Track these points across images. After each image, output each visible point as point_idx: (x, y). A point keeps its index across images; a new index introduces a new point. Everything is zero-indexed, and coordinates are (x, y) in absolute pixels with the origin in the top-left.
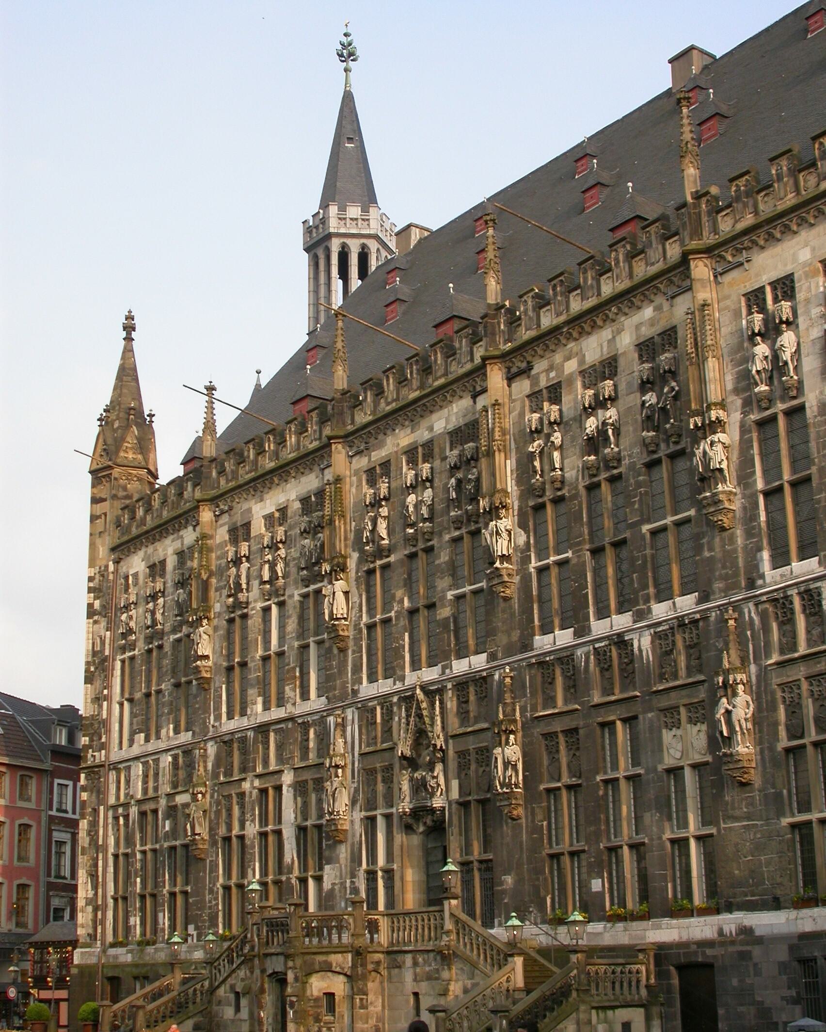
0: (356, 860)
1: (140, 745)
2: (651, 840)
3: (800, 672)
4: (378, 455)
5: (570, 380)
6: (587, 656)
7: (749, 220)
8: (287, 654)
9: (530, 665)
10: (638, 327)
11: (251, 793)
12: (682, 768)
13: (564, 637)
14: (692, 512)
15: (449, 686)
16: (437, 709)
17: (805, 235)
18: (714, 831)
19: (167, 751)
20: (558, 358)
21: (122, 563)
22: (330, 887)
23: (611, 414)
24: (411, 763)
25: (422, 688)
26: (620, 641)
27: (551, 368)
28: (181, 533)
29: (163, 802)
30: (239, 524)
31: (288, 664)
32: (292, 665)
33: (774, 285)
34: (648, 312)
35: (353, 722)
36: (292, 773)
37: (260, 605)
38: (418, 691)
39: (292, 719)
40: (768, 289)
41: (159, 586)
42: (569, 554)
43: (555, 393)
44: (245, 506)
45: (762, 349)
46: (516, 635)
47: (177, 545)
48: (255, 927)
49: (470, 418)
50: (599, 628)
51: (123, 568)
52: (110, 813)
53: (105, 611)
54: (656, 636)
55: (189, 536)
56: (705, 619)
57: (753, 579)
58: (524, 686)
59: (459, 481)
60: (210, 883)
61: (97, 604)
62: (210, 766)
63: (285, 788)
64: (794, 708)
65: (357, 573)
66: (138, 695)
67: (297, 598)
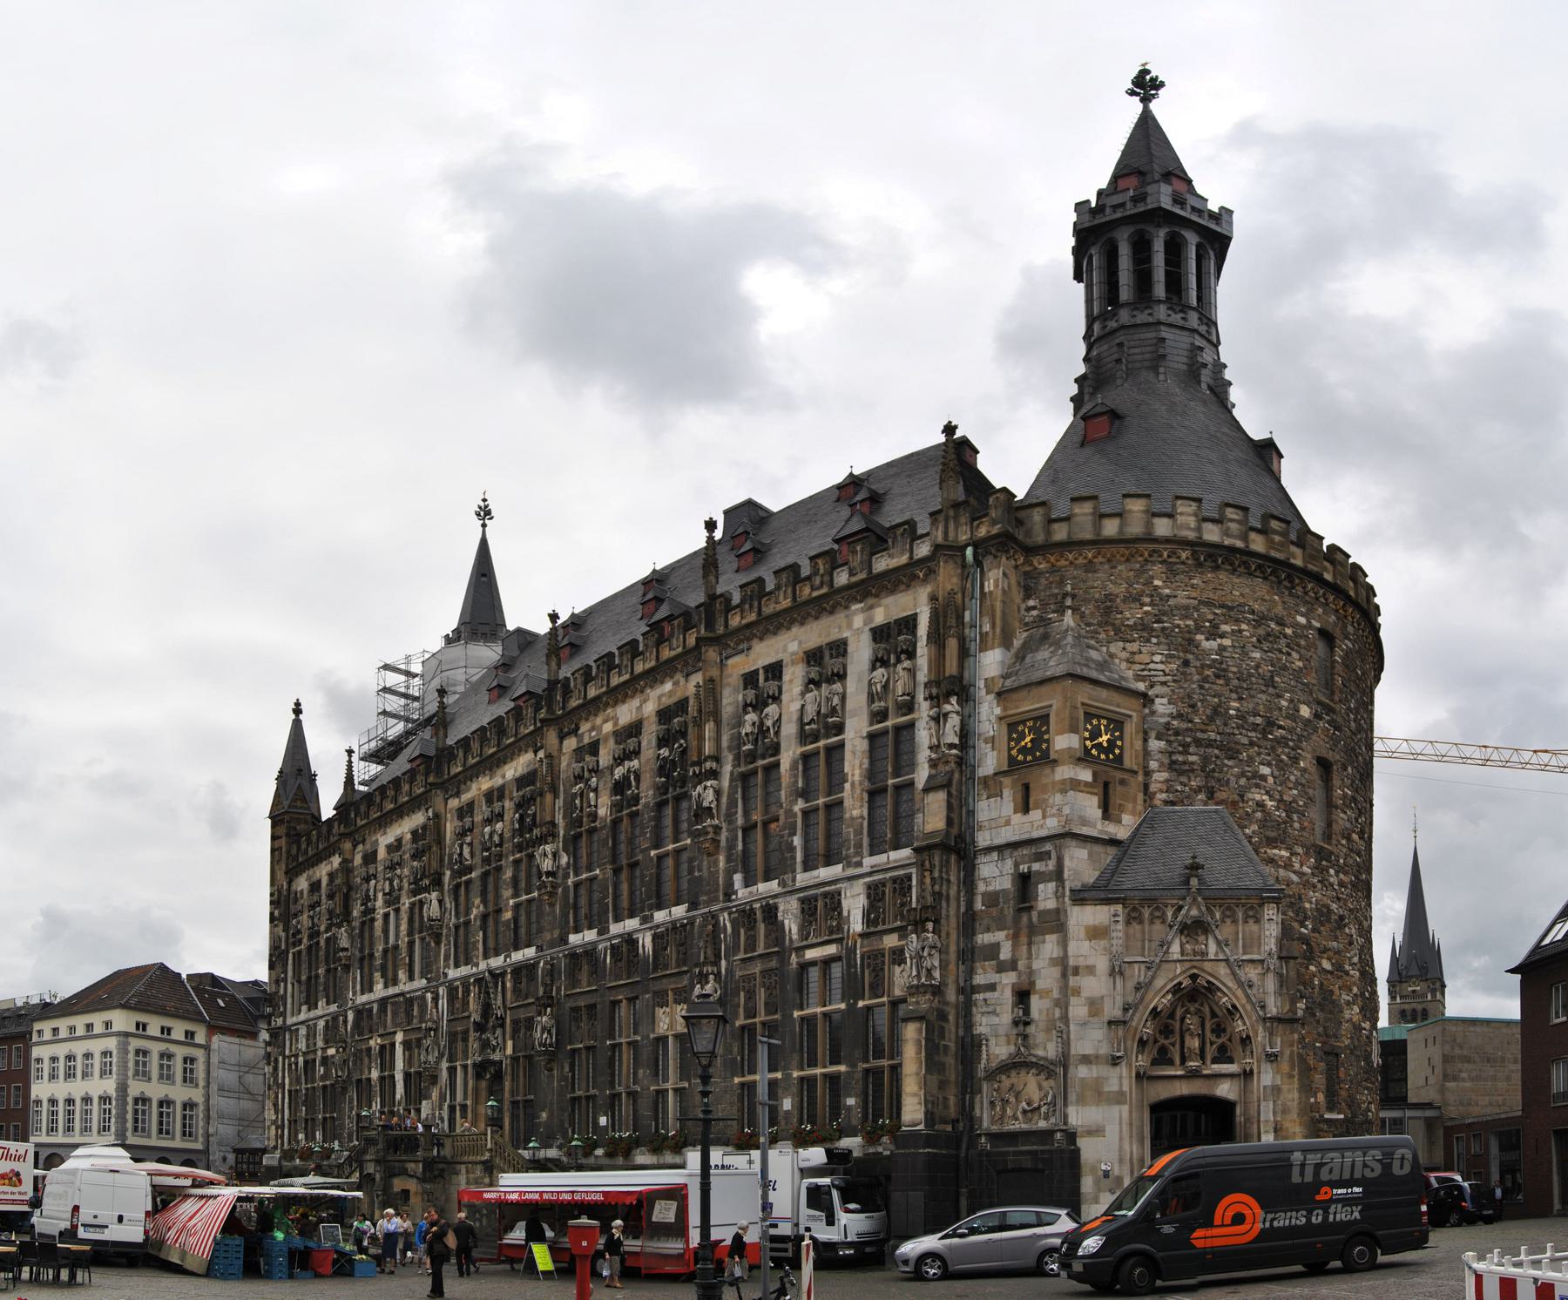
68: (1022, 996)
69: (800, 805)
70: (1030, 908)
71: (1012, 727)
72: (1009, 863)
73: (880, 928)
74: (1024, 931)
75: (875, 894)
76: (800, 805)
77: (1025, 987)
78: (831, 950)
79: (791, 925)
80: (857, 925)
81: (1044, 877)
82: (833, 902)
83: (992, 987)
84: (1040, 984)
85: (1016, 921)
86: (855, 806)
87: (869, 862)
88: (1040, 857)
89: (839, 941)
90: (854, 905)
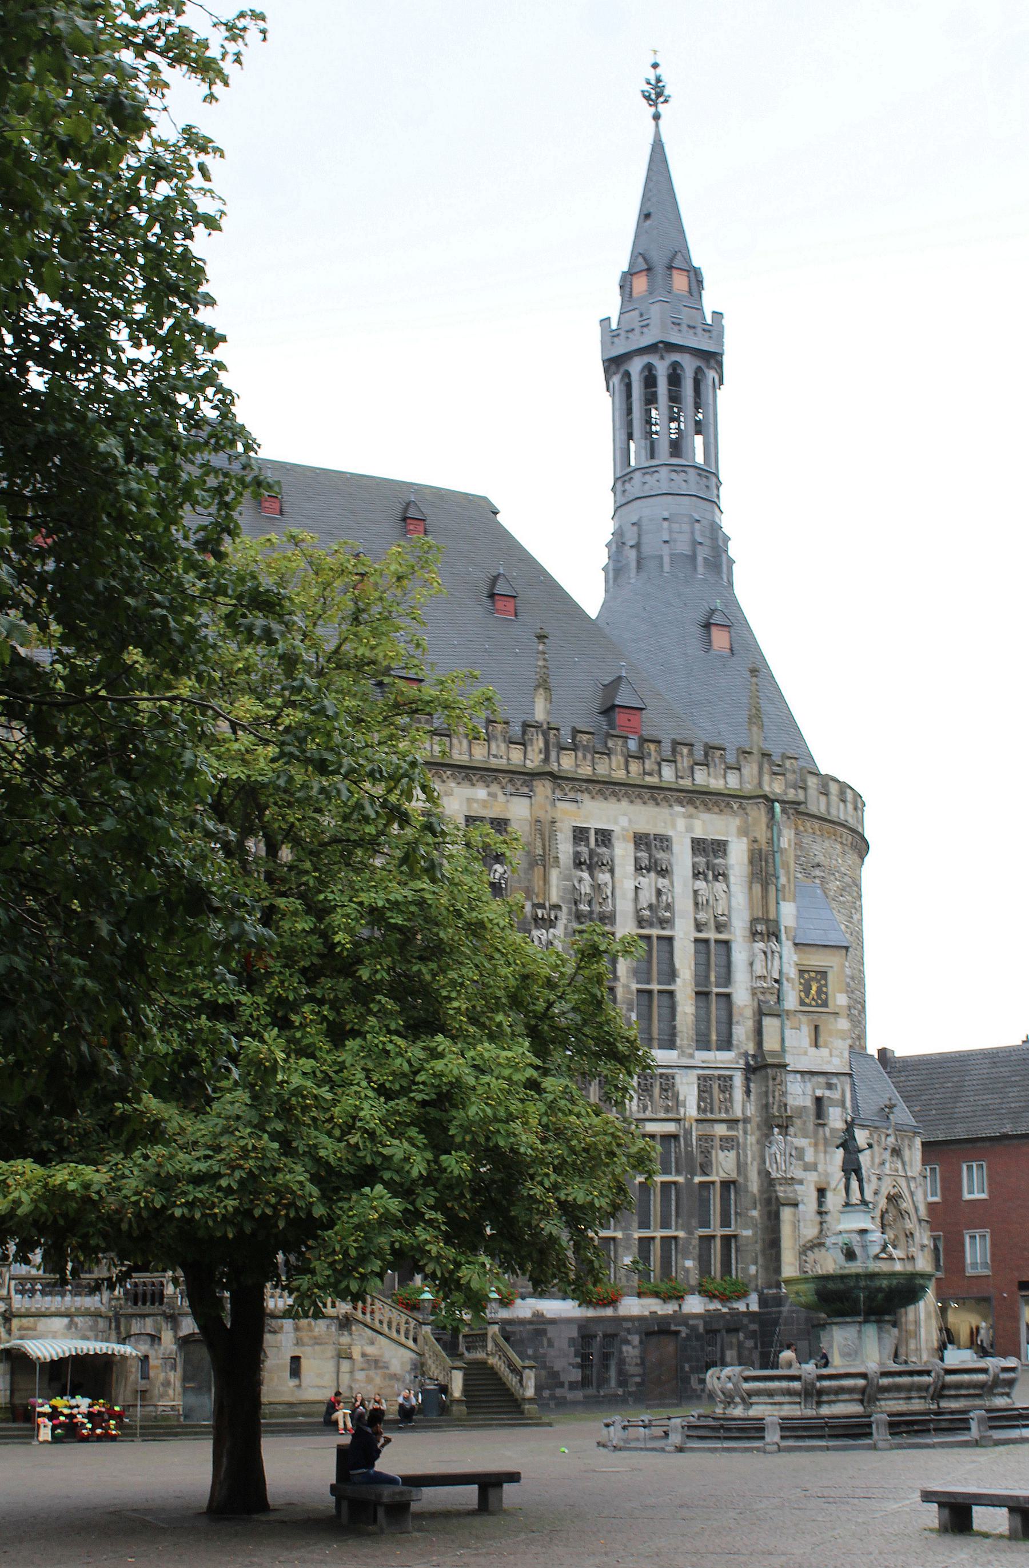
7: (586, 771)
10: (470, 801)
17: (624, 804)
33: (597, 831)
34: (481, 793)
40: (592, 832)
45: (586, 875)
68: (821, 1192)
69: (635, 986)
70: (824, 1125)
71: (801, 972)
72: (809, 1086)
73: (709, 1116)
74: (821, 1141)
75: (705, 1085)
77: (823, 1186)
78: (671, 1128)
80: (691, 1110)
81: (833, 1103)
83: (801, 1182)
84: (833, 1185)
85: (816, 1133)
86: (686, 1007)
87: (702, 1057)
88: (830, 1086)
90: (688, 1089)
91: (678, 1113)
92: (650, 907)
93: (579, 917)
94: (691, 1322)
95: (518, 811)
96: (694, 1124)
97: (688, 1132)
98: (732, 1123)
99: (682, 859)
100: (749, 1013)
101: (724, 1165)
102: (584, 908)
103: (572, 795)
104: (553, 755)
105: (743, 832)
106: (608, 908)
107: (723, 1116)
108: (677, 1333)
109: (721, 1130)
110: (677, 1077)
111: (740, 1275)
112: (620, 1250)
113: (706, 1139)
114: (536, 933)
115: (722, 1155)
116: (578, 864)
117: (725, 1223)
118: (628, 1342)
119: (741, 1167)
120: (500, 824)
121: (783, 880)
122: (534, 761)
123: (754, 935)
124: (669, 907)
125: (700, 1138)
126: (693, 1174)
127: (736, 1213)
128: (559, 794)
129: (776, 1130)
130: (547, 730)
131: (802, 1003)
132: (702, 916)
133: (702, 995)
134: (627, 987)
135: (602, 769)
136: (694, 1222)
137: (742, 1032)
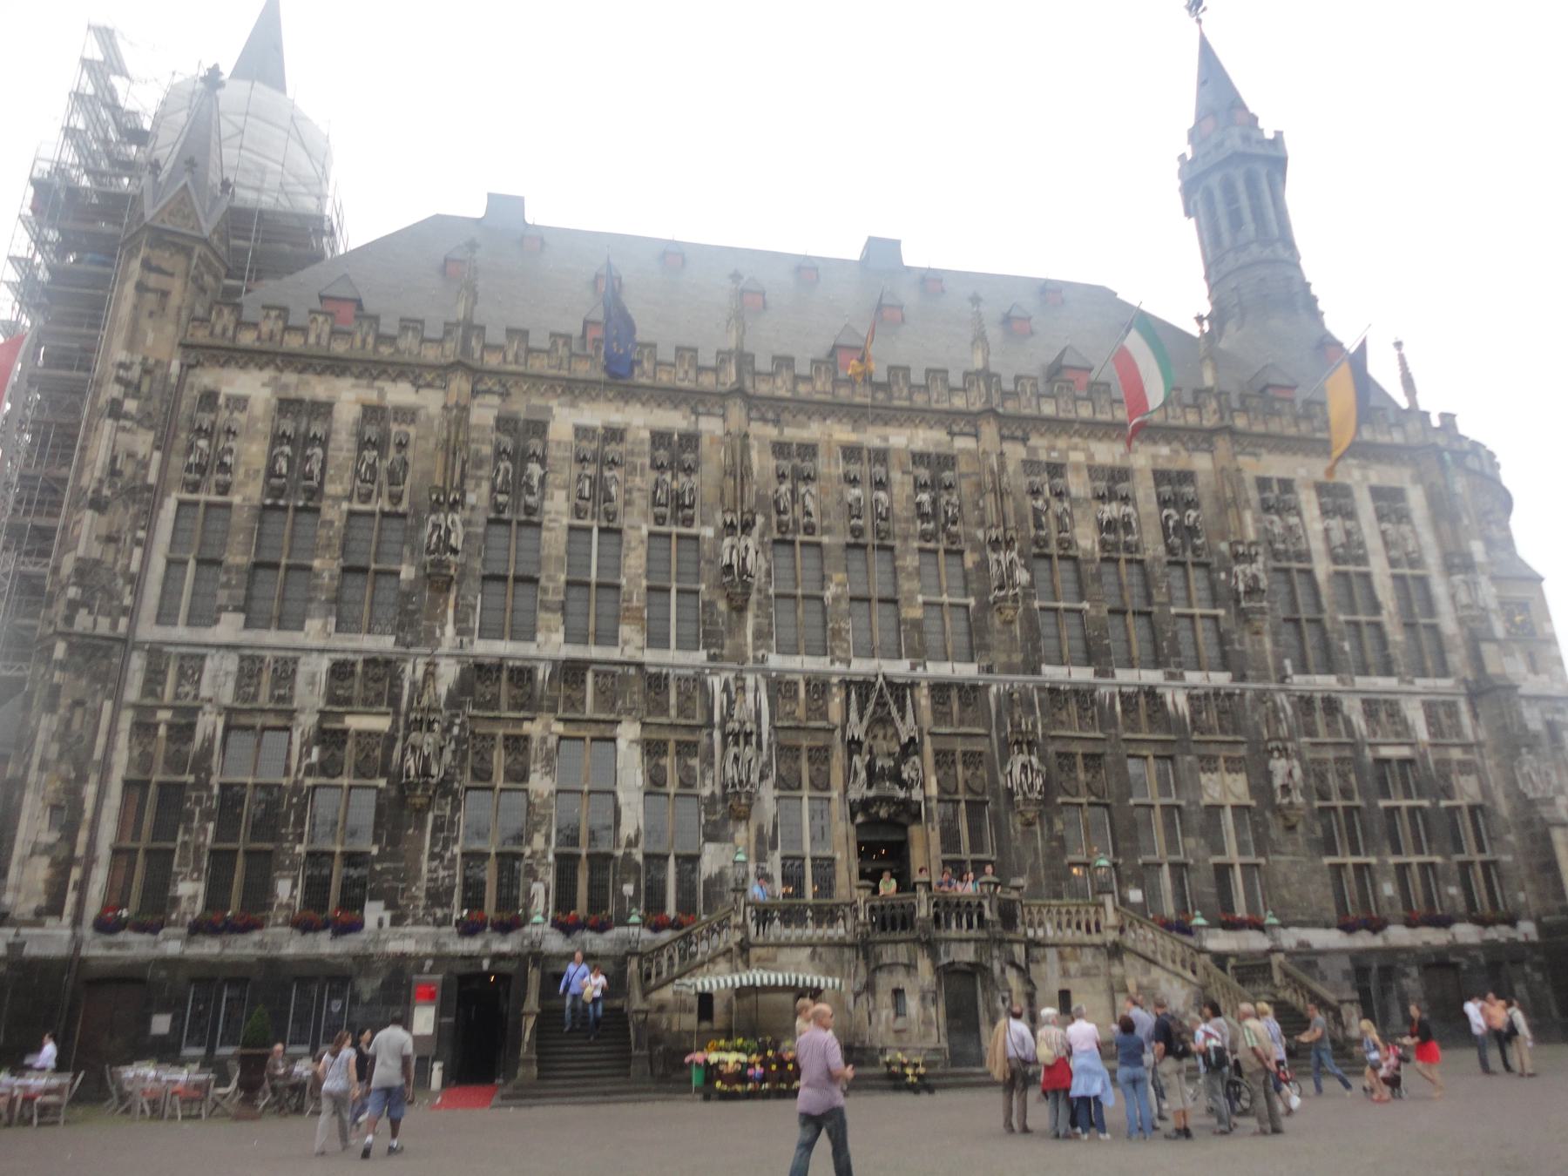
0: (764, 844)
1: (229, 628)
2: (1197, 861)
3: (1330, 754)
4: (793, 434)
5: (1077, 467)
6: (1112, 697)
7: (1259, 428)
8: (624, 589)
9: (1040, 689)
11: (544, 740)
12: (1222, 807)
13: (1083, 675)
14: (1221, 612)
15: (924, 684)
16: (909, 702)
17: (1299, 458)
18: (1262, 861)
19: (322, 651)
20: (1061, 443)
21: (198, 371)
22: (715, 870)
23: (1130, 509)
24: (853, 746)
25: (885, 677)
26: (1151, 693)
27: (1053, 448)
28: (378, 383)
29: (307, 722)
30: (522, 416)
31: (630, 600)
32: (635, 603)
34: (1164, 450)
35: (757, 689)
36: (638, 726)
37: (565, 521)
38: (881, 679)
39: (640, 666)
41: (317, 429)
42: (1086, 605)
43: (1056, 470)
44: (536, 401)
45: (1275, 518)
46: (1018, 658)
47: (372, 396)
48: (749, 909)
49: (943, 450)
50: (1127, 677)
51: (206, 378)
52: (127, 718)
53: (145, 420)
54: (1190, 698)
55: (399, 394)
56: (1242, 695)
57: (1283, 678)
58: (1032, 705)
59: (934, 502)
60: (433, 845)
61: (131, 405)
62: (443, 690)
63: (622, 744)
64: (1322, 777)
65: (762, 535)
66: (237, 557)
67: (644, 531)
69: (1342, 618)
75: (1430, 709)
76: (1342, 618)
78: (1405, 752)
79: (1359, 721)
80: (1422, 733)
82: (1394, 712)
86: (1396, 635)
87: (1420, 683)
89: (1411, 745)
90: (1415, 714)
91: (1409, 736)
92: (1342, 545)
93: (1276, 555)
94: (1472, 953)
95: (1202, 463)
96: (1429, 750)
97: (1424, 756)
98: (1467, 747)
99: (1365, 507)
100: (1459, 641)
101: (1467, 790)
102: (1280, 546)
103: (1249, 449)
104: (1227, 416)
105: (1418, 479)
106: (1303, 547)
107: (1455, 740)
108: (1455, 966)
109: (1456, 754)
110: (1403, 705)
111: (1509, 901)
112: (1377, 876)
113: (1443, 763)
114: (1238, 569)
115: (1462, 779)
116: (1267, 508)
117: (1481, 849)
118: (1406, 975)
119: (1485, 789)
120: (1187, 477)
121: (1466, 521)
122: (1210, 421)
123: (1449, 568)
124: (1361, 545)
125: (1437, 763)
126: (1438, 799)
127: (1490, 838)
128: (1237, 449)
129: (1524, 750)
130: (1219, 395)
131: (1508, 632)
132: (1394, 553)
133: (1410, 626)
134: (1334, 620)
135: (1275, 426)
136: (1449, 847)
137: (1457, 659)
